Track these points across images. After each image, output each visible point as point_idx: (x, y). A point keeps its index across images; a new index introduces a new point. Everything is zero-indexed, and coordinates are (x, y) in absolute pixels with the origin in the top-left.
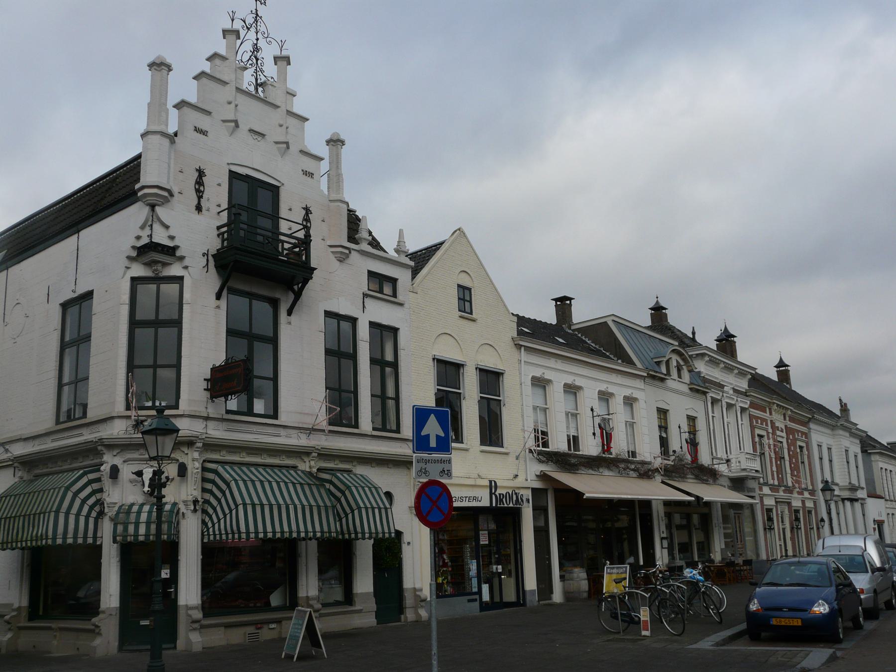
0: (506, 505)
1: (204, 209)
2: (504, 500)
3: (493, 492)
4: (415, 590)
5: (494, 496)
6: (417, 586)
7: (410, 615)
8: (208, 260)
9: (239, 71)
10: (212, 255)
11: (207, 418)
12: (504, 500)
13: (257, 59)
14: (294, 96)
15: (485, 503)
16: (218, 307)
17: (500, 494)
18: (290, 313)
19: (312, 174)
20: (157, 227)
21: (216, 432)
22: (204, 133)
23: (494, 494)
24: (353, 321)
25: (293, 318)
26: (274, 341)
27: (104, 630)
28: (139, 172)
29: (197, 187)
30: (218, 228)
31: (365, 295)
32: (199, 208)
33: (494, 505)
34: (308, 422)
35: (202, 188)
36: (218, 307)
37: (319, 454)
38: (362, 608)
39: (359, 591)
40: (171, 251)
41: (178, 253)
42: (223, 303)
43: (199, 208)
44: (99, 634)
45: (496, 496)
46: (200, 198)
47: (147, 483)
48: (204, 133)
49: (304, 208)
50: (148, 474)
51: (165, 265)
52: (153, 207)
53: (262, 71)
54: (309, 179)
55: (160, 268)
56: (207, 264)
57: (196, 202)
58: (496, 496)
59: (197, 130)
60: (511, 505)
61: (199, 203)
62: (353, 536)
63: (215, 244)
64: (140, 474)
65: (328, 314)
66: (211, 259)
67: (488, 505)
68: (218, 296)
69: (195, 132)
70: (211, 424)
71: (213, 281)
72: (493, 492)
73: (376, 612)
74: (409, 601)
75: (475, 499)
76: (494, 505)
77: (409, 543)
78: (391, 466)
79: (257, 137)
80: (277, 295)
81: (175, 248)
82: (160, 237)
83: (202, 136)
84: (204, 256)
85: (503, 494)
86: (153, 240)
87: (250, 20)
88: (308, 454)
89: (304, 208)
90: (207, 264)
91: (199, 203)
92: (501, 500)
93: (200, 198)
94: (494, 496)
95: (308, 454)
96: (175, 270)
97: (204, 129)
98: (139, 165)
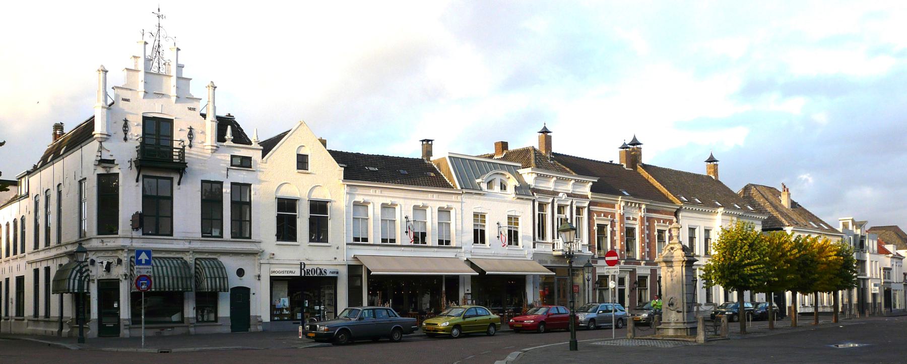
0: (311, 275)
1: (128, 139)
2: (310, 273)
3: (303, 268)
4: (256, 316)
5: (303, 271)
6: (258, 315)
7: (252, 329)
8: (131, 164)
9: (148, 62)
10: (134, 161)
11: (132, 238)
12: (310, 273)
13: (159, 52)
14: (183, 67)
15: (297, 274)
16: (137, 186)
17: (307, 270)
18: (179, 184)
19: (195, 109)
20: (103, 152)
21: (138, 244)
22: (128, 100)
23: (303, 269)
24: (221, 183)
25: (181, 186)
26: (171, 198)
27: (91, 327)
28: (94, 125)
29: (124, 129)
30: (137, 147)
31: (228, 169)
32: (125, 139)
33: (303, 275)
34: (191, 236)
35: (127, 129)
36: (137, 186)
37: (193, 252)
38: (221, 324)
39: (220, 316)
40: (112, 162)
41: (115, 163)
42: (140, 183)
43: (125, 139)
44: (90, 329)
45: (305, 271)
46: (126, 134)
47: (104, 267)
48: (128, 100)
49: (189, 128)
50: (105, 263)
51: (110, 168)
52: (101, 142)
53: (162, 58)
54: (192, 111)
55: (108, 170)
56: (131, 166)
57: (124, 136)
58: (305, 271)
59: (123, 100)
60: (316, 275)
61: (125, 137)
62: (218, 290)
63: (134, 155)
64: (102, 263)
65: (203, 181)
66: (133, 163)
67: (299, 275)
68: (137, 181)
69: (122, 101)
70: (134, 240)
71: (134, 172)
72: (303, 268)
73: (231, 326)
74: (252, 322)
75: (291, 272)
76: (303, 275)
77: (254, 294)
78: (242, 255)
79: (159, 95)
80: (172, 176)
81: (114, 160)
82: (106, 156)
83: (126, 102)
84: (129, 162)
85: (310, 270)
86: (102, 158)
87: (155, 31)
88: (188, 252)
89: (189, 128)
90: (131, 166)
91: (125, 137)
92: (308, 273)
93: (126, 134)
94: (303, 271)
95: (188, 252)
96: (115, 170)
97: (127, 98)
98: (94, 120)
